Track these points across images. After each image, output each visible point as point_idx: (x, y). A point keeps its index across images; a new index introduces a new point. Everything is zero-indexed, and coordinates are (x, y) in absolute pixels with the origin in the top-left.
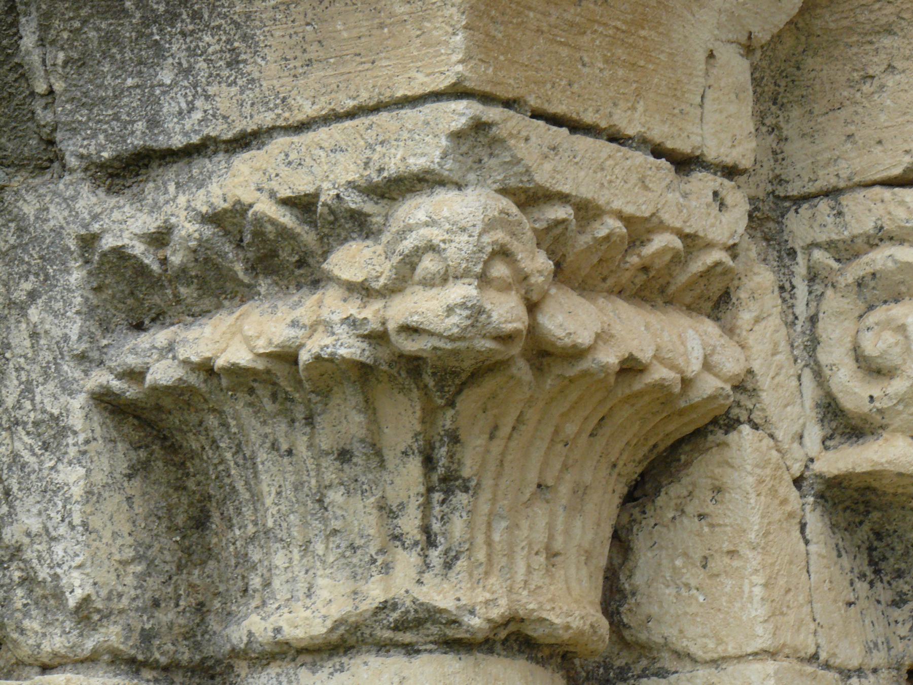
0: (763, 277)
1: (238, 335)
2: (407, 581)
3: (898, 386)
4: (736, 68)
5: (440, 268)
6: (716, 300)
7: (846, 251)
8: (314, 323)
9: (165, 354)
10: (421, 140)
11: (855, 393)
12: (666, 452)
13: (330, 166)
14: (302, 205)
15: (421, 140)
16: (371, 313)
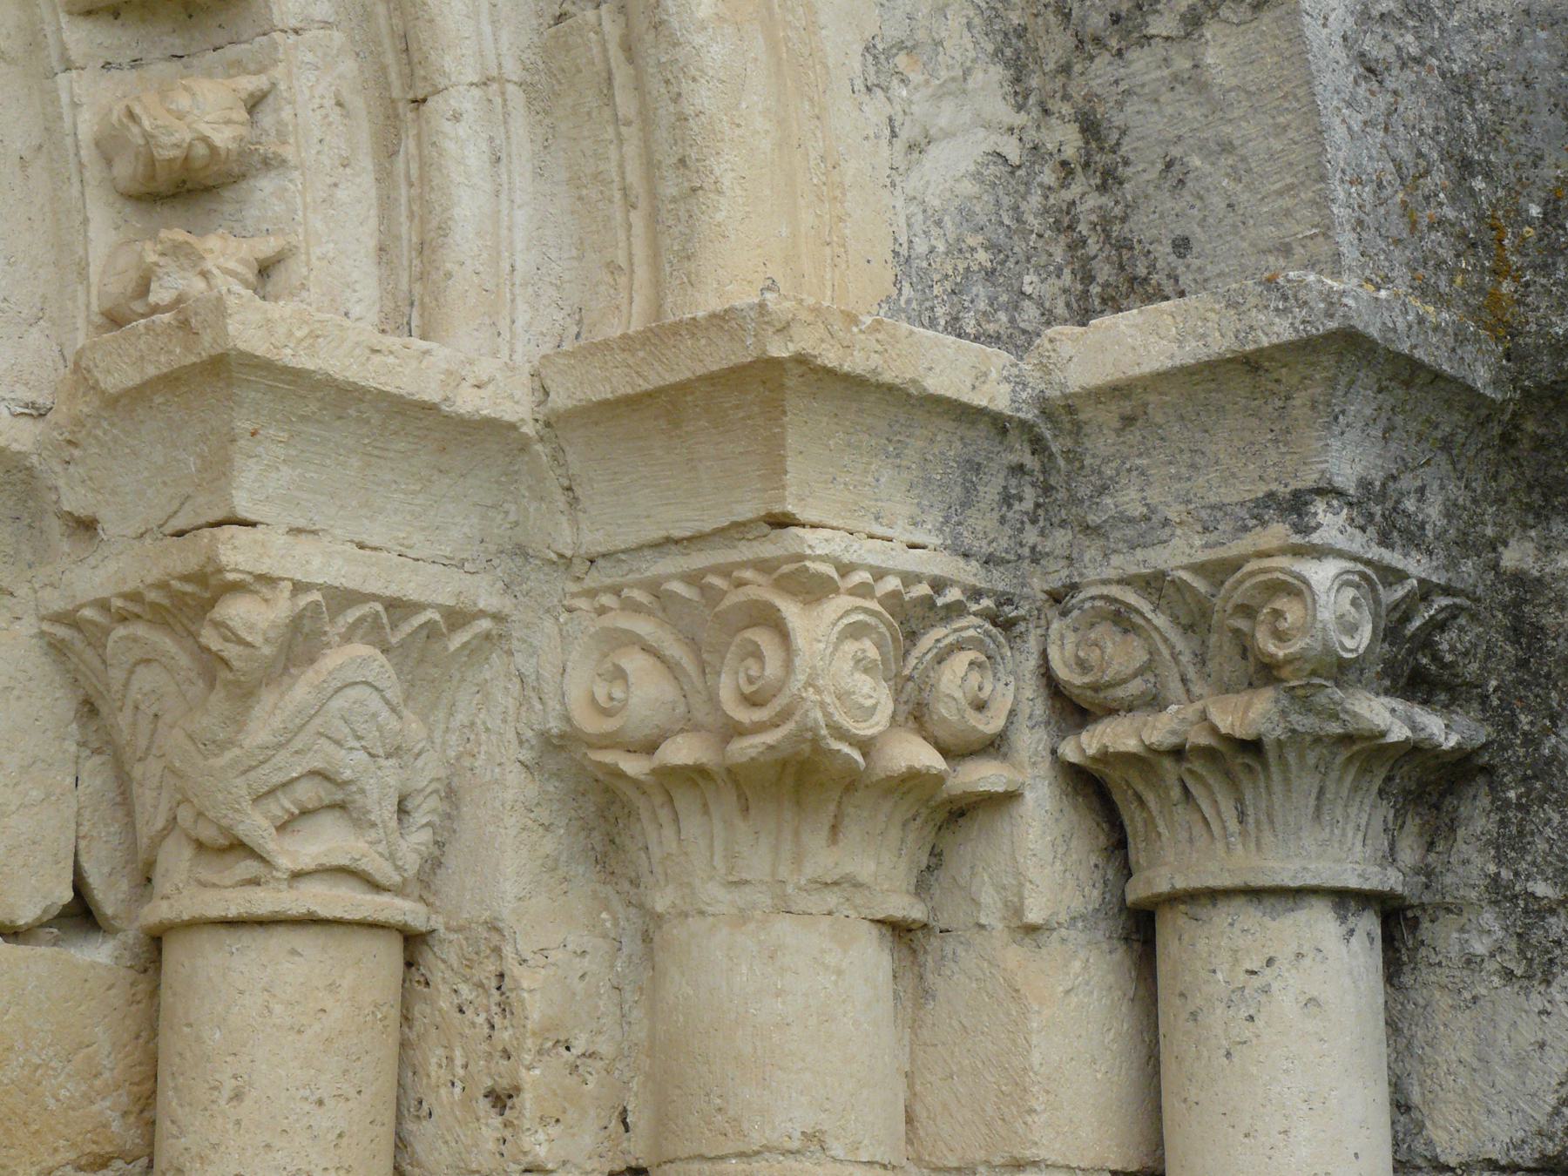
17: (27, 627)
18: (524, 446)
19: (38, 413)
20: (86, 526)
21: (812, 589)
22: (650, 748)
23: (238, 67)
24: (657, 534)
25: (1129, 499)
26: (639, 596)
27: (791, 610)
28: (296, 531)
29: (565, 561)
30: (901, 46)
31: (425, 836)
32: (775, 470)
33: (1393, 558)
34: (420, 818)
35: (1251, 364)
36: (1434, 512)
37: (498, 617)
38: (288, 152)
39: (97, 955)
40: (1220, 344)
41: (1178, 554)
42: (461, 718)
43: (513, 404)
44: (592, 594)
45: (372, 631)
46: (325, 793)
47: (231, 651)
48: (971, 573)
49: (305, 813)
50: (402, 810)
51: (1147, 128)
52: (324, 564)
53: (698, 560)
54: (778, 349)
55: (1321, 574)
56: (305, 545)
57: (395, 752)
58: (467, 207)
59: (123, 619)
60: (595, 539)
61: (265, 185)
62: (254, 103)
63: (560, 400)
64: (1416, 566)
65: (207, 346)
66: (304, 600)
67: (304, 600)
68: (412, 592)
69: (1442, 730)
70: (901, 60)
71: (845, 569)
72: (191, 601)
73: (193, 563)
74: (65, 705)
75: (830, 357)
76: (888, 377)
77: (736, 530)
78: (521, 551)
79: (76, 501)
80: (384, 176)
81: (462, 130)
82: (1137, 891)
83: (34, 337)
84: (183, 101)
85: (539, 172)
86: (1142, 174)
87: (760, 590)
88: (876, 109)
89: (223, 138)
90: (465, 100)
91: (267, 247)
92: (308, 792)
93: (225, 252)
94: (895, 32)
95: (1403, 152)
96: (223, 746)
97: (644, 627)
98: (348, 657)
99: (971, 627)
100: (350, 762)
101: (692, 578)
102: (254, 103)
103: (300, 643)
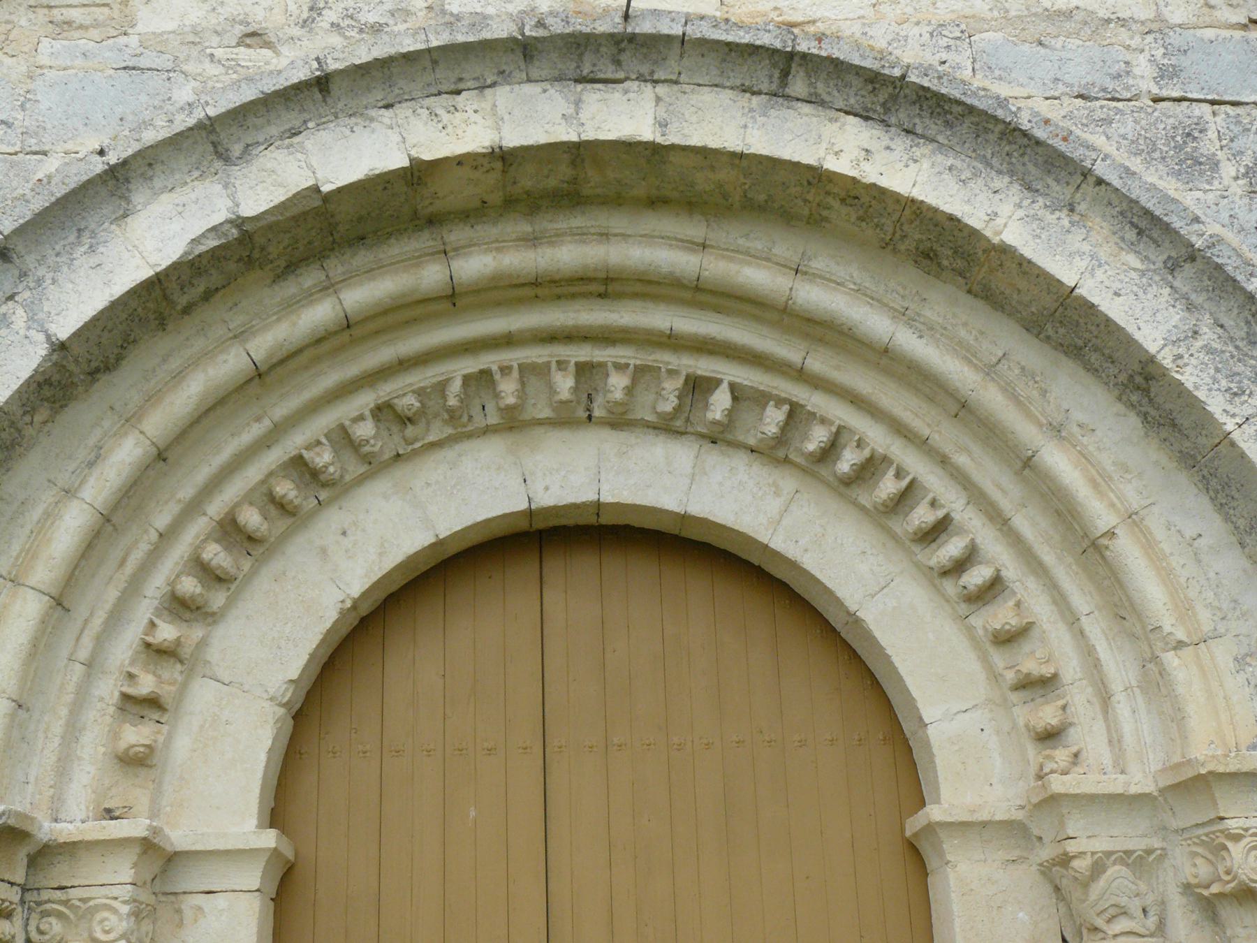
0: (19, 909)
3: (47, 937)
4: (25, 860)
7: (39, 904)
17: (1035, 868)
18: (1155, 798)
19: (1023, 807)
20: (1040, 838)
21: (1237, 838)
22: (1208, 887)
23: (1059, 697)
24: (1193, 823)
26: (1196, 841)
27: (1229, 845)
28: (1089, 837)
29: (1177, 831)
30: (1247, 655)
31: (1156, 918)
32: (1215, 804)
34: (1151, 913)
37: (1162, 849)
38: (1075, 720)
42: (1161, 880)
43: (1150, 788)
44: (1185, 840)
45: (1122, 861)
46: (1119, 911)
47: (1077, 875)
49: (1114, 917)
50: (1144, 910)
52: (1101, 845)
53: (1207, 830)
54: (1203, 771)
56: (1093, 841)
57: (1137, 895)
58: (1127, 728)
59: (1054, 865)
60: (1182, 825)
61: (1072, 730)
62: (1064, 708)
63: (1161, 785)
65: (1049, 793)
66: (1096, 857)
67: (1096, 857)
68: (1131, 847)
70: (1248, 660)
71: (1246, 830)
72: (1065, 860)
73: (1061, 851)
74: (1050, 889)
75: (1221, 769)
76: (1244, 770)
77: (1211, 822)
78: (1165, 828)
79: (1036, 832)
80: (1106, 719)
81: (1121, 706)
83: (1021, 783)
84: (1041, 714)
85: (1149, 712)
87: (1222, 840)
88: (1241, 678)
89: (1054, 722)
91: (1074, 749)
92: (1112, 911)
93: (1061, 755)
94: (1244, 651)
96: (1084, 901)
97: (1199, 850)
98: (1113, 870)
100: (1123, 901)
101: (1207, 835)
102: (1064, 708)
103: (1098, 869)
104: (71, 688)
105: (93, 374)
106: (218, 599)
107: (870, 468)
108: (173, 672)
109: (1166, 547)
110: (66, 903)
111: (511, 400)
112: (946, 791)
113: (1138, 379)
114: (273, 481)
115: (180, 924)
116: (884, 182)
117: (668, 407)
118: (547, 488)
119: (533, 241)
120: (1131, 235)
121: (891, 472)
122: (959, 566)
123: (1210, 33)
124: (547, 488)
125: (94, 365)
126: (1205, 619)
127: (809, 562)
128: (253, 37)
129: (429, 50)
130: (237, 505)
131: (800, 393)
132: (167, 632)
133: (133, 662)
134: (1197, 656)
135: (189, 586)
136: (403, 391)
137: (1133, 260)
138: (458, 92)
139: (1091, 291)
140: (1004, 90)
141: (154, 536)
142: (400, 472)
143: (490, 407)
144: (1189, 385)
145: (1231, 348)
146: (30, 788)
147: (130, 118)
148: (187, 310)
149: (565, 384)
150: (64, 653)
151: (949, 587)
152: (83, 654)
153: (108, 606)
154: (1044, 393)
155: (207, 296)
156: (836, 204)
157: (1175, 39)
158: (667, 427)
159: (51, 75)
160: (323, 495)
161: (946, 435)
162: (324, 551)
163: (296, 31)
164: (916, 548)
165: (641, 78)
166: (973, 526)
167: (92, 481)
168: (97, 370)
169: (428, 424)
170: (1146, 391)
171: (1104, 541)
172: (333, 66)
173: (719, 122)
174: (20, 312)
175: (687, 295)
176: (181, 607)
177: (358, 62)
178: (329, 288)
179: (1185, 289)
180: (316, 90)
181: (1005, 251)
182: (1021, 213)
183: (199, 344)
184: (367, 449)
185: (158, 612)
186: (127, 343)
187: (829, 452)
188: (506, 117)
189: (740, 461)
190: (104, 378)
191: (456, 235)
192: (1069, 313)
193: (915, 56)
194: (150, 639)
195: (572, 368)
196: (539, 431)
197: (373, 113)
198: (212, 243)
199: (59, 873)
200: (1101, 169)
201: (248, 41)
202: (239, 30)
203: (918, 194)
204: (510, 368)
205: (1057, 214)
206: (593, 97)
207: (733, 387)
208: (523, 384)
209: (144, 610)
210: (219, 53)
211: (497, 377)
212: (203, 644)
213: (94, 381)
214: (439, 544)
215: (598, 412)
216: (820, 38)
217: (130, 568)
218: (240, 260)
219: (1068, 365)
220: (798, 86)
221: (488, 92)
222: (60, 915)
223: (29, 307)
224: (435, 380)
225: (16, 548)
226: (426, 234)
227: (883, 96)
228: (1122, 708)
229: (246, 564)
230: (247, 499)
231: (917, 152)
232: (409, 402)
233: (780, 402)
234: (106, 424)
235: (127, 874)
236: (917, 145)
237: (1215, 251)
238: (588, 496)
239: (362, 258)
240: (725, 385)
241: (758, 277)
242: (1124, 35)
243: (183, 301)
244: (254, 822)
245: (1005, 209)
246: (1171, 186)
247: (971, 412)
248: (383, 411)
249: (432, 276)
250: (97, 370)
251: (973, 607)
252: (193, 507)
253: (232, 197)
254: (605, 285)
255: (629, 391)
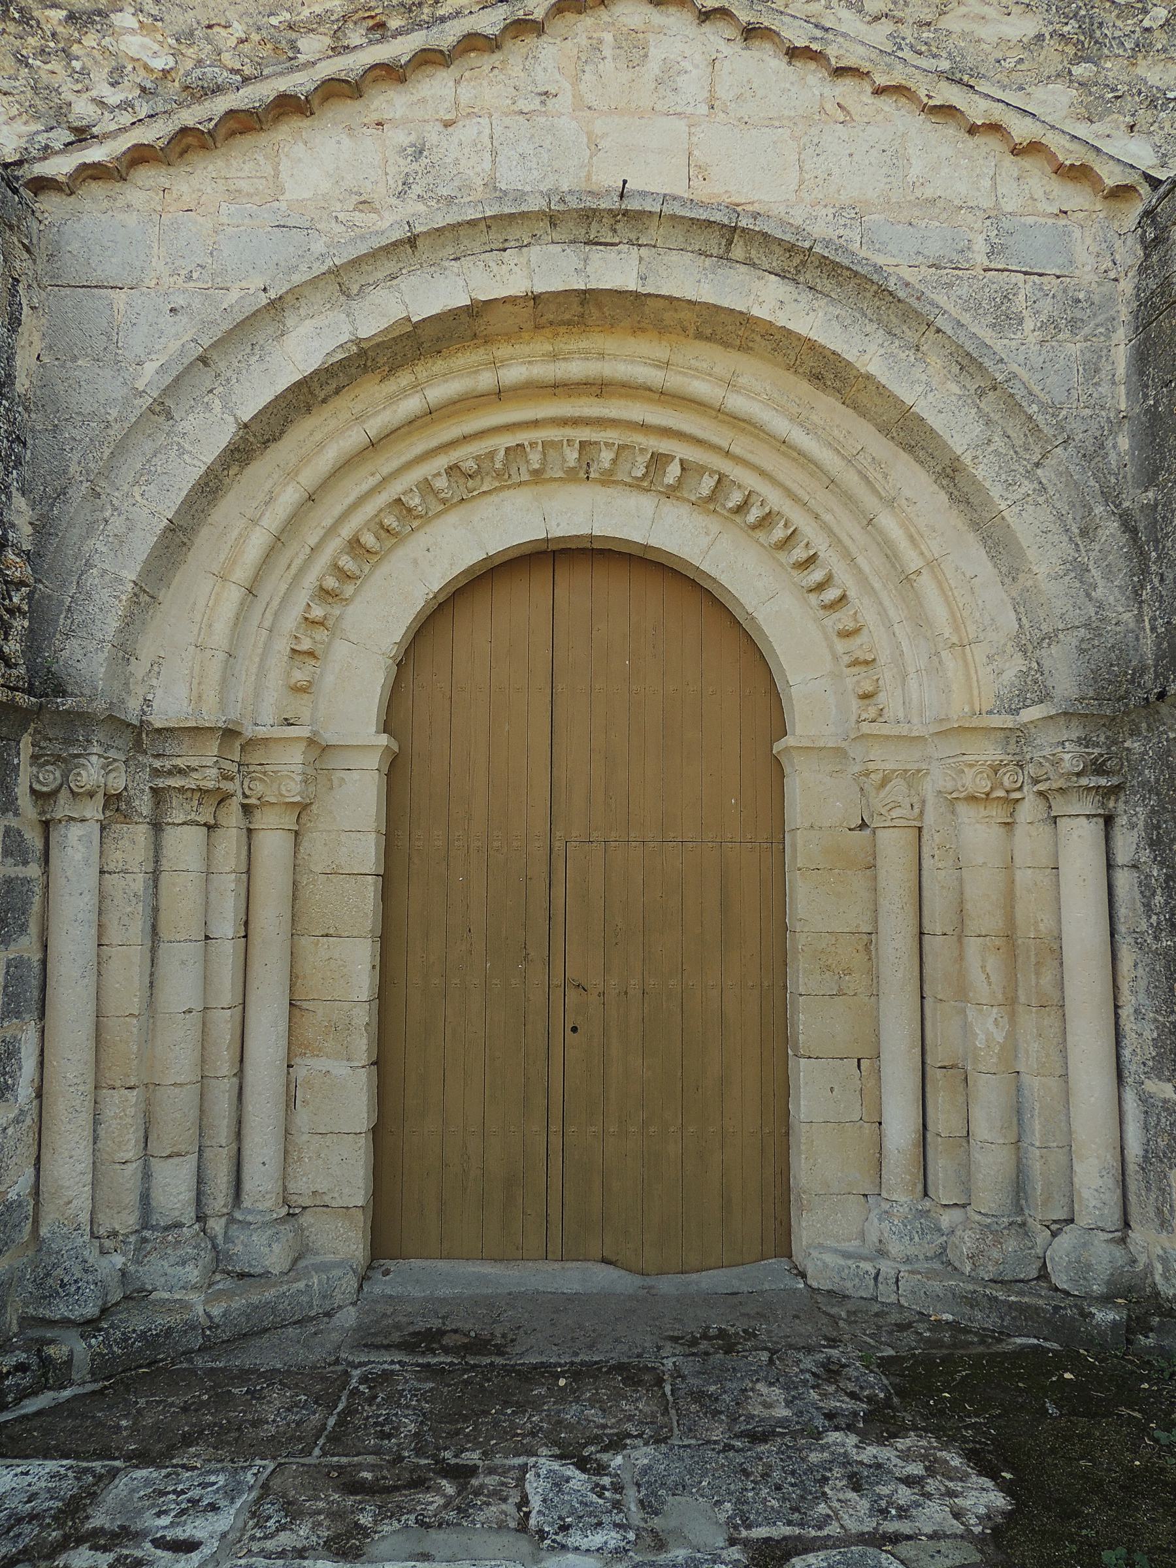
1: (176, 782)
2: (193, 816)
5: (209, 779)
6: (232, 779)
7: (249, 773)
8: (189, 783)
9: (161, 783)
10: (210, 762)
11: (248, 792)
12: (223, 799)
13: (194, 763)
14: (188, 767)
15: (210, 762)
16: (198, 783)
25: (1038, 742)
33: (1090, 750)
34: (915, 807)
35: (1051, 717)
36: (1102, 739)
39: (868, 832)
40: (1045, 715)
41: (1047, 752)
48: (1010, 757)
51: (1047, 664)
52: (889, 766)
55: (1067, 757)
64: (1097, 751)
69: (1103, 781)
82: (1053, 814)
86: (1046, 672)
88: (989, 669)
90: (914, 676)
92: (892, 805)
95: (1093, 667)
99: (1011, 767)
100: (900, 799)
104: (261, 645)
105: (266, 443)
106: (349, 589)
107: (766, 521)
108: (321, 634)
109: (953, 584)
110: (265, 773)
111: (537, 466)
112: (799, 730)
113: (948, 470)
114: (382, 515)
115: (331, 788)
116: (791, 326)
117: (639, 473)
118: (558, 525)
119: (554, 357)
120: (956, 369)
121: (782, 523)
122: (820, 587)
123: (1030, 220)
124: (558, 525)
125: (266, 437)
126: (972, 629)
127: (724, 579)
128: (364, 204)
129: (485, 218)
130: (360, 530)
131: (726, 466)
132: (317, 612)
133: (297, 628)
134: (964, 653)
135: (331, 583)
136: (465, 455)
137: (955, 388)
138: (505, 250)
139: (923, 409)
140: (880, 260)
141: (308, 550)
142: (462, 510)
143: (523, 470)
144: (980, 478)
145: (1012, 452)
146: (239, 705)
147: (283, 264)
148: (324, 401)
149: (572, 456)
150: (256, 623)
151: (813, 598)
152: (267, 624)
153: (281, 594)
154: (886, 476)
155: (337, 391)
156: (758, 338)
157: (1006, 224)
158: (637, 485)
159: (230, 230)
160: (415, 524)
161: (821, 498)
162: (415, 562)
163: (394, 201)
164: (794, 573)
165: (630, 243)
166: (831, 559)
167: (268, 514)
168: (268, 440)
169: (482, 479)
170: (953, 479)
171: (913, 577)
172: (419, 229)
173: (685, 277)
174: (217, 401)
175: (657, 396)
176: (325, 594)
177: (436, 226)
178: (417, 387)
179: (987, 410)
180: (407, 246)
181: (869, 377)
182: (882, 351)
183: (332, 424)
184: (443, 495)
185: (312, 598)
186: (286, 423)
187: (742, 508)
188: (537, 269)
189: (684, 510)
190: (273, 446)
191: (503, 351)
192: (907, 423)
193: (821, 228)
194: (307, 615)
195: (577, 445)
196: (555, 485)
197: (446, 264)
198: (340, 356)
199: (256, 757)
200: (940, 322)
201: (361, 207)
202: (355, 199)
203: (813, 335)
204: (536, 443)
205: (907, 352)
206: (597, 255)
207: (681, 461)
208: (544, 454)
209: (303, 597)
210: (341, 216)
211: (528, 449)
212: (339, 618)
213: (266, 448)
214: (489, 558)
215: (592, 475)
216: (756, 216)
217: (294, 570)
218: (359, 366)
219: (905, 456)
220: (738, 252)
221: (525, 249)
222: (261, 780)
223: (223, 398)
224: (487, 451)
225: (222, 557)
226: (482, 351)
227: (796, 261)
228: (913, 684)
229: (366, 568)
230: (367, 525)
231: (816, 304)
232: (470, 465)
233: (712, 472)
234: (275, 476)
235: (299, 759)
236: (816, 299)
237: (1010, 384)
238: (585, 531)
239: (439, 366)
240: (677, 460)
241: (701, 388)
242: (970, 218)
243: (322, 395)
244: (374, 729)
245: (872, 348)
246: (987, 335)
247: (837, 486)
248: (453, 470)
249: (485, 380)
250: (268, 440)
251: (828, 613)
252: (332, 530)
253: (353, 323)
254: (600, 388)
255: (614, 461)
